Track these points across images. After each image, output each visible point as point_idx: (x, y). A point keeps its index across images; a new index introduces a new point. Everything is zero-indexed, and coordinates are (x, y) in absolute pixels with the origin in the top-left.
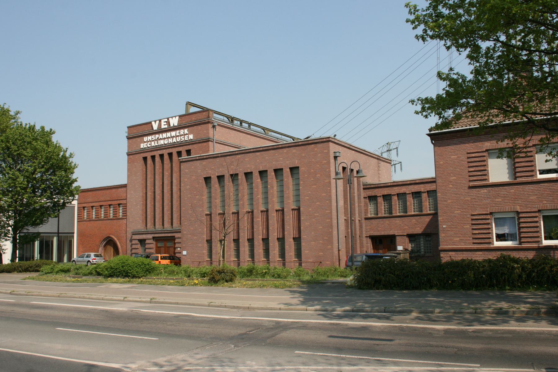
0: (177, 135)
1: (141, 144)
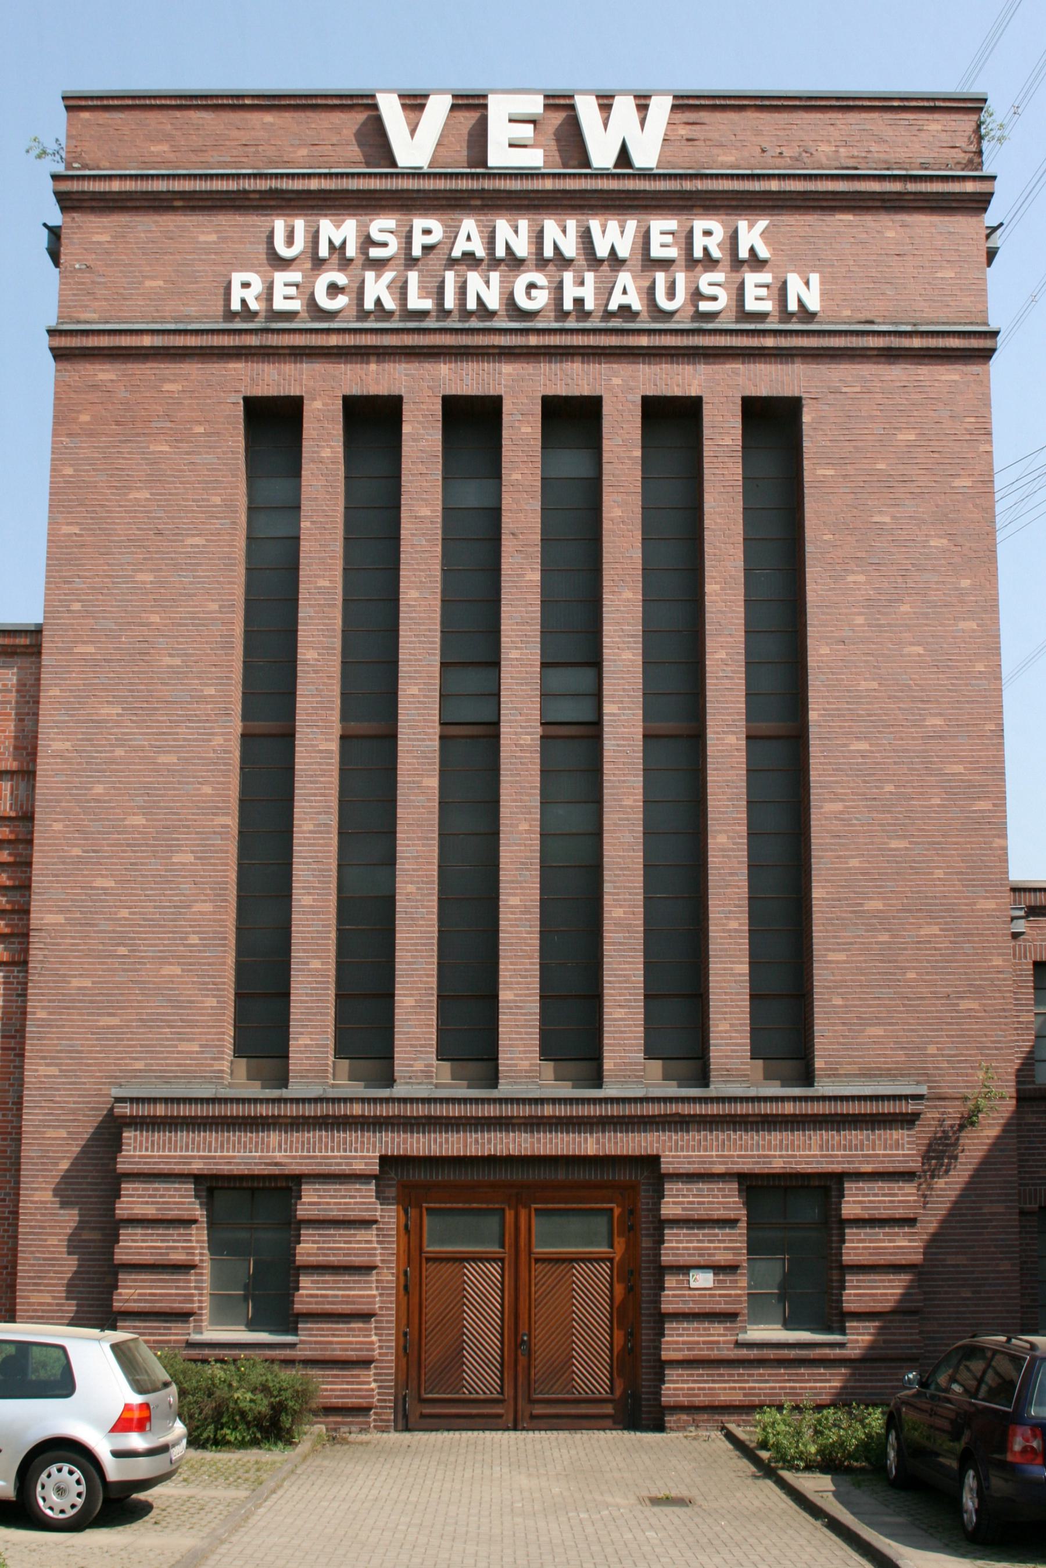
1: (237, 278)
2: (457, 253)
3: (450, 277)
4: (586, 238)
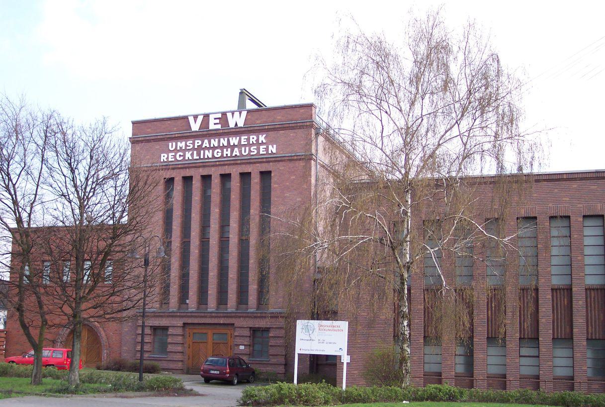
0: (242, 143)
1: (162, 155)
2: (203, 147)
3: (202, 152)
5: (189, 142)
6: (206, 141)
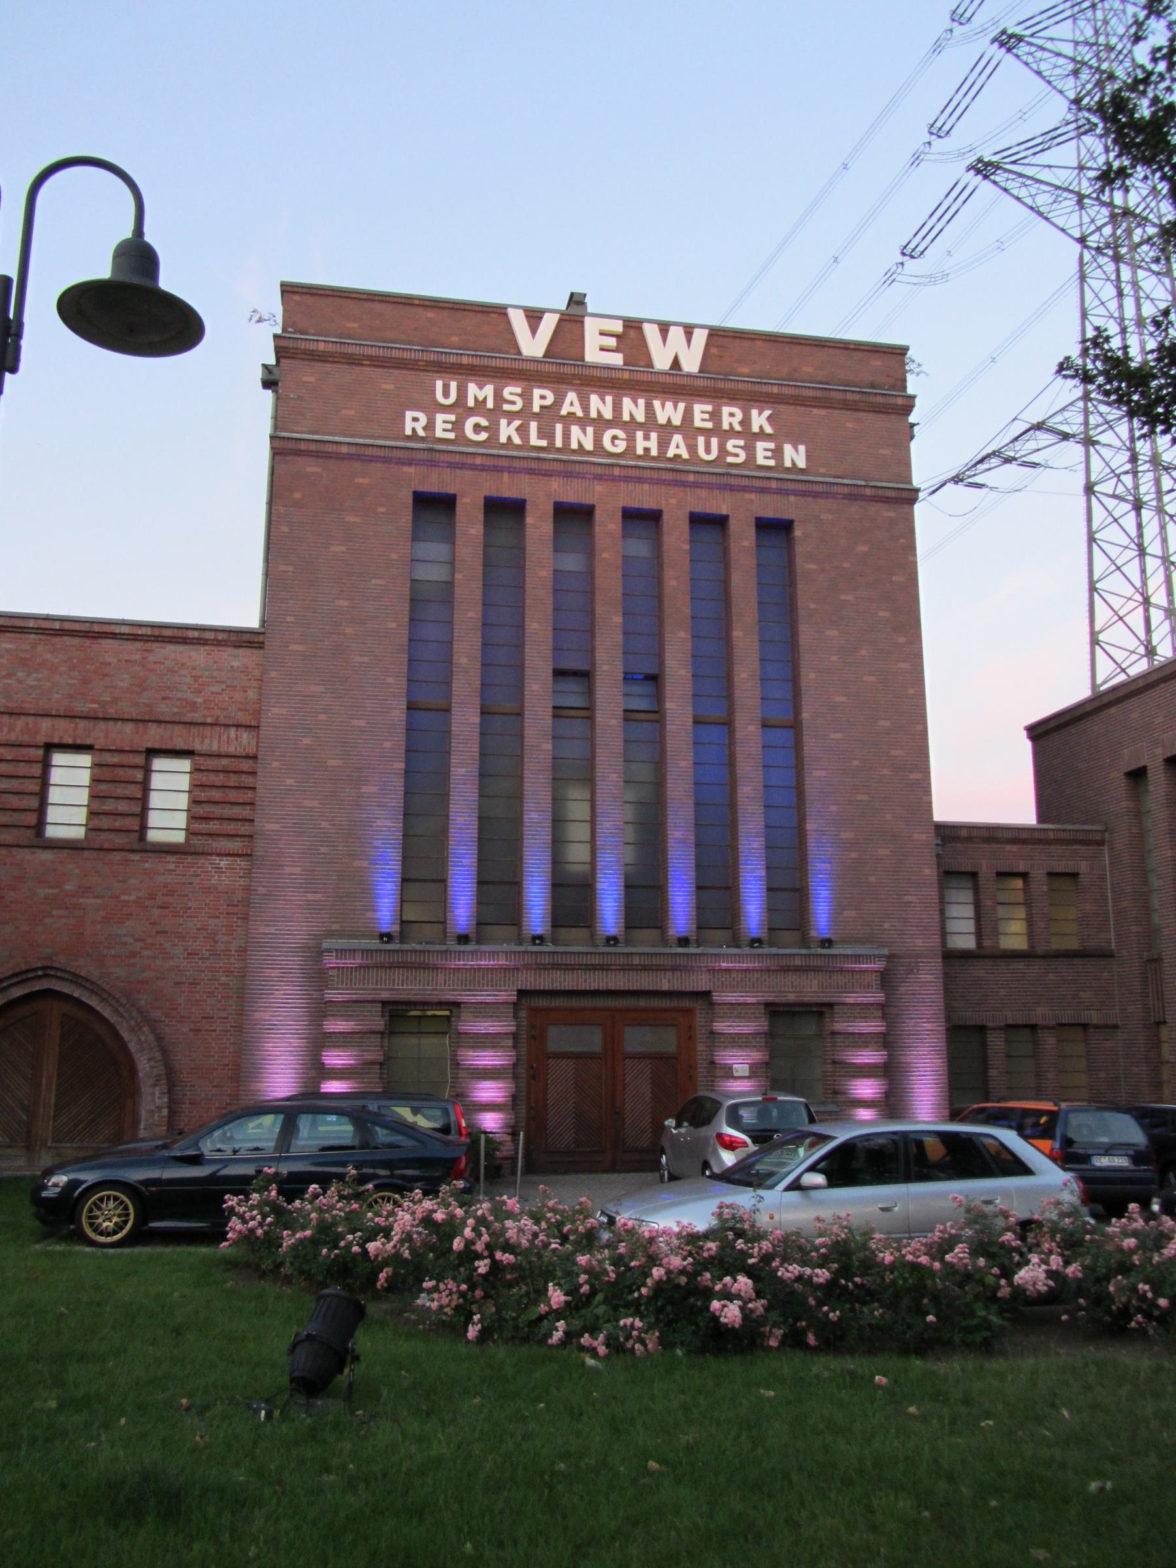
1: (409, 415)
2: (564, 412)
3: (559, 428)
4: (650, 410)
5: (511, 391)
6: (572, 396)
